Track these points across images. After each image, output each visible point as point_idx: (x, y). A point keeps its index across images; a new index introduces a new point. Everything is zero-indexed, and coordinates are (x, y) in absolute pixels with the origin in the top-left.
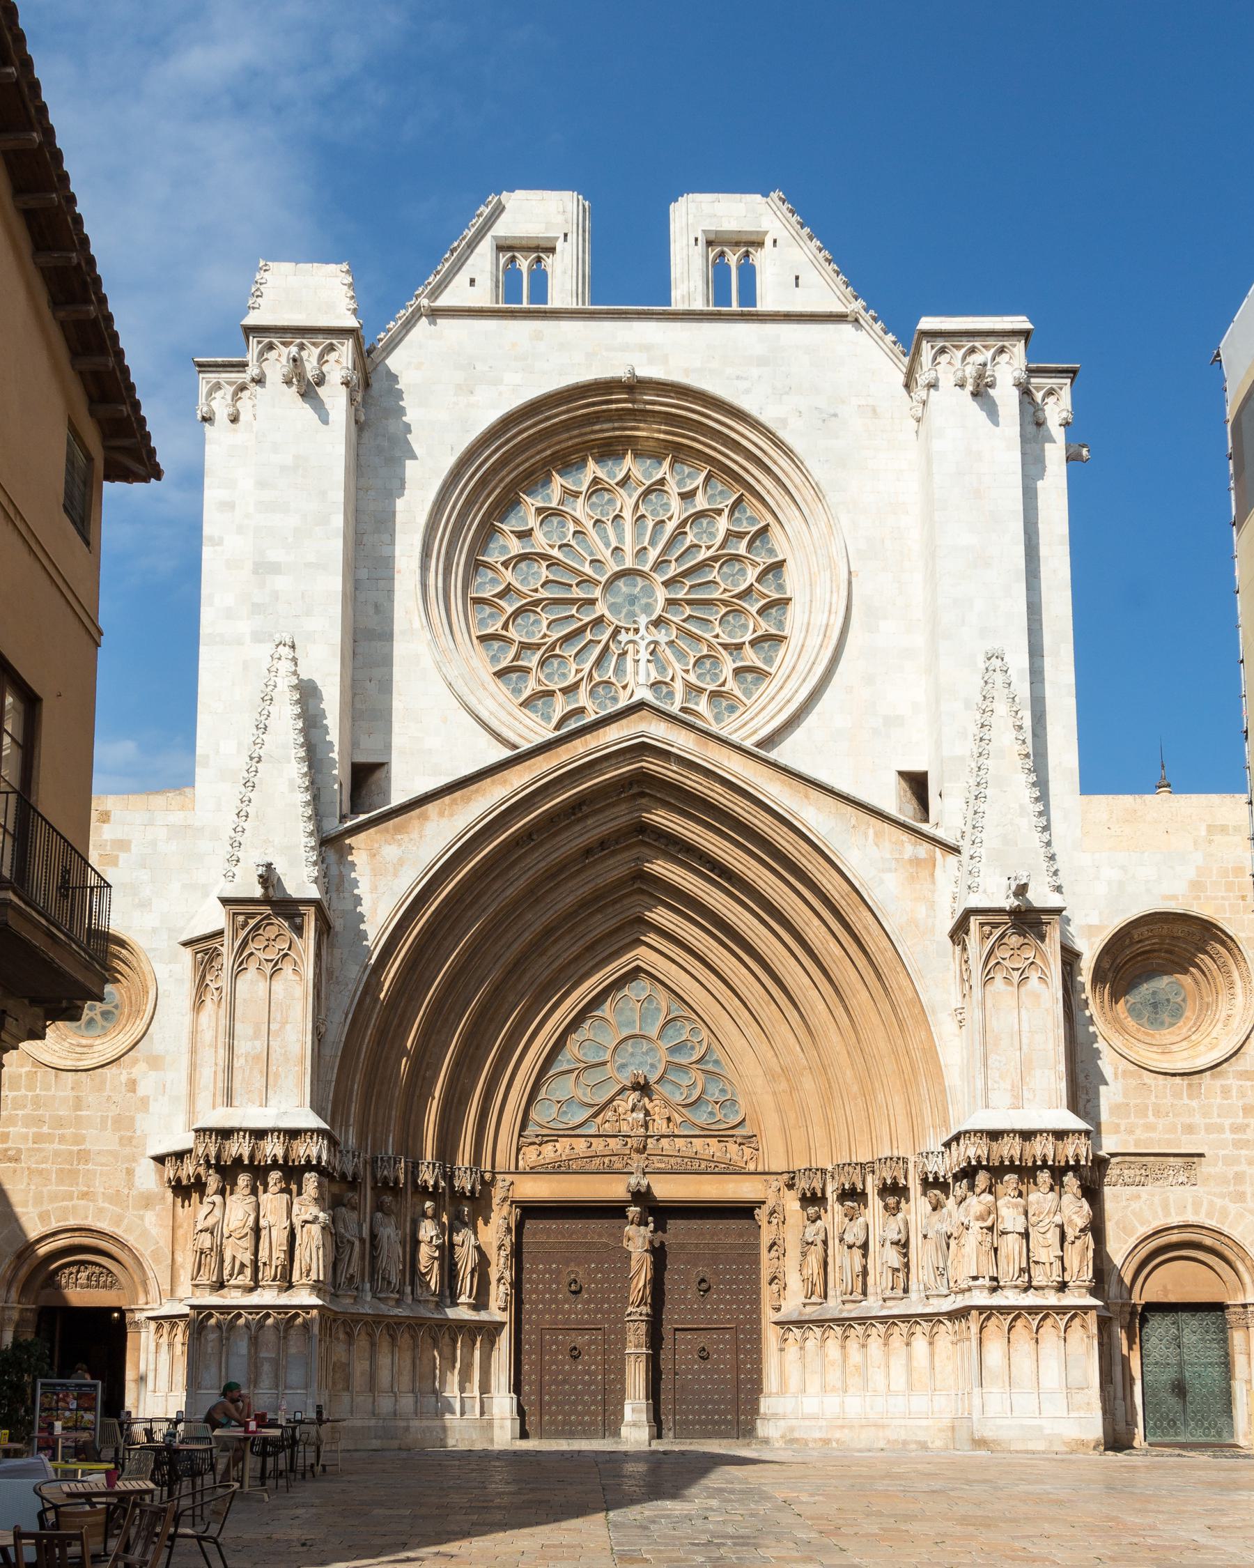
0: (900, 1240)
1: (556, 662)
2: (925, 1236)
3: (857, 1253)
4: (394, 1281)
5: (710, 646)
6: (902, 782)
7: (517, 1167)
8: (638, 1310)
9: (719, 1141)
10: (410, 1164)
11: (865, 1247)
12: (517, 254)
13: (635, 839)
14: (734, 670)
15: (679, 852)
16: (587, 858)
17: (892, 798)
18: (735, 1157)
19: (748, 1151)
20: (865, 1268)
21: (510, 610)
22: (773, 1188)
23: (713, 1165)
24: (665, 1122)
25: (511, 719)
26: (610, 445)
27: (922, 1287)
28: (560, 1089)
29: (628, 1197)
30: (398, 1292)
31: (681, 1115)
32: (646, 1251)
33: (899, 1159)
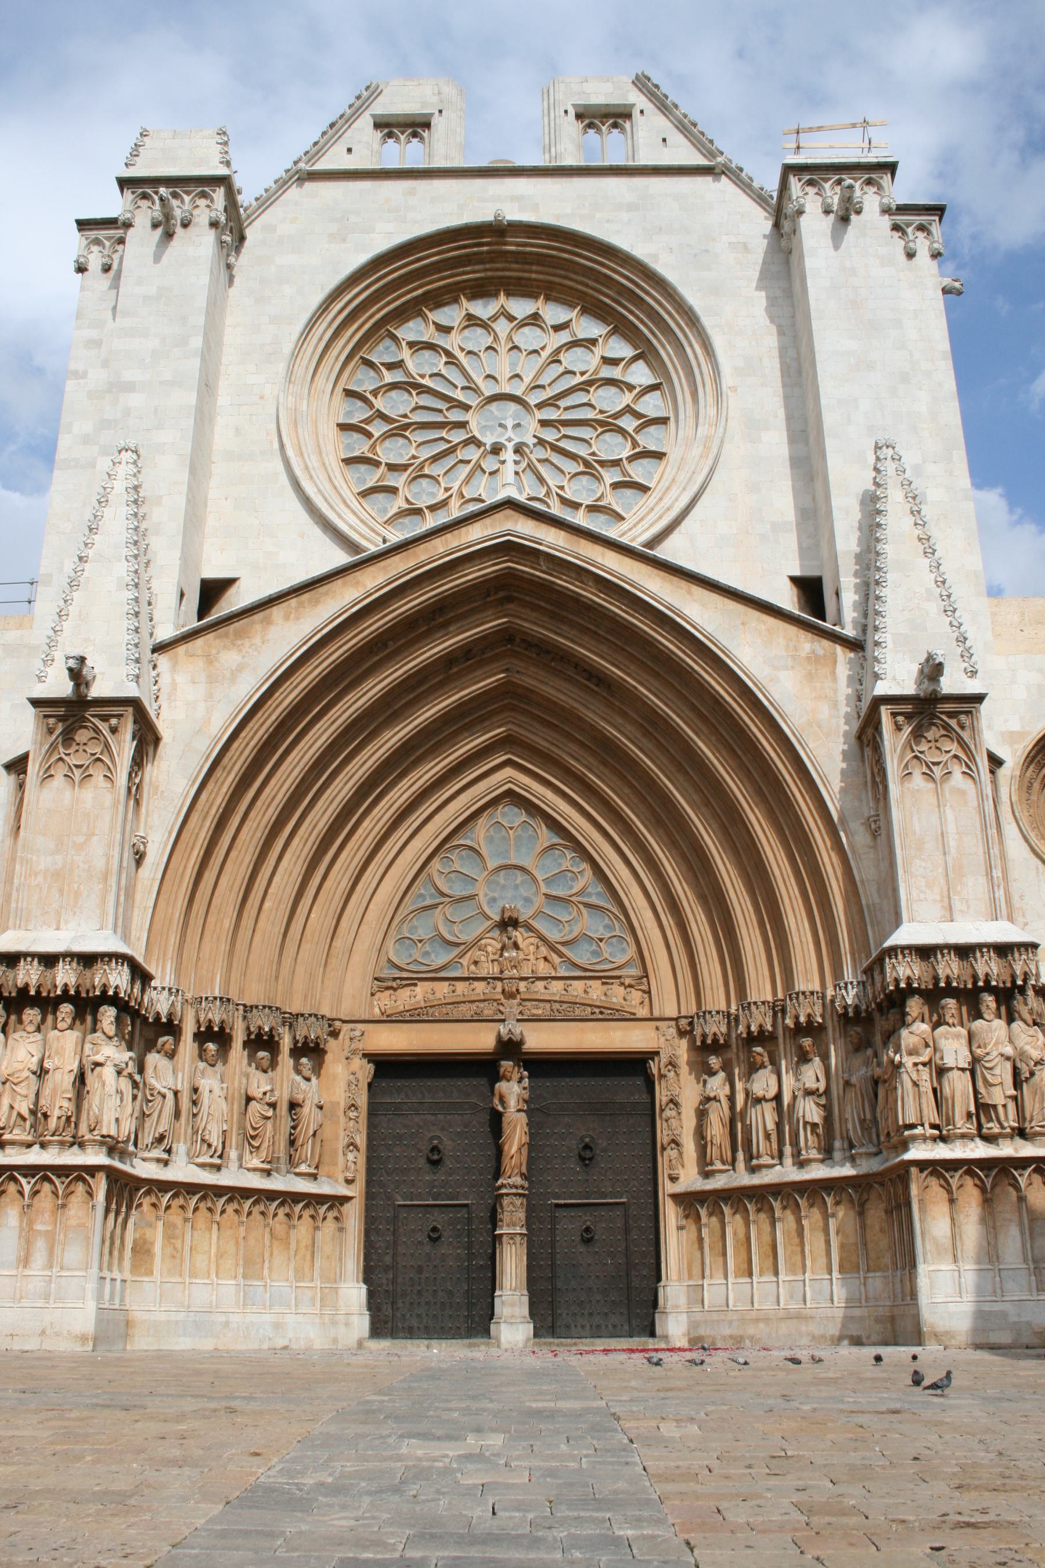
0: (818, 1089)
1: (424, 482)
2: (847, 1084)
4: (215, 1144)
5: (587, 464)
6: (795, 590)
8: (509, 1181)
9: (604, 983)
10: (241, 1008)
11: (778, 1098)
12: (395, 130)
13: (504, 648)
14: (611, 485)
15: (552, 660)
16: (450, 668)
17: (787, 599)
19: (636, 996)
21: (377, 435)
23: (597, 1010)
25: (373, 534)
26: (482, 286)
27: (846, 1145)
30: (221, 1157)
31: (561, 955)
32: (519, 1111)
33: (812, 993)
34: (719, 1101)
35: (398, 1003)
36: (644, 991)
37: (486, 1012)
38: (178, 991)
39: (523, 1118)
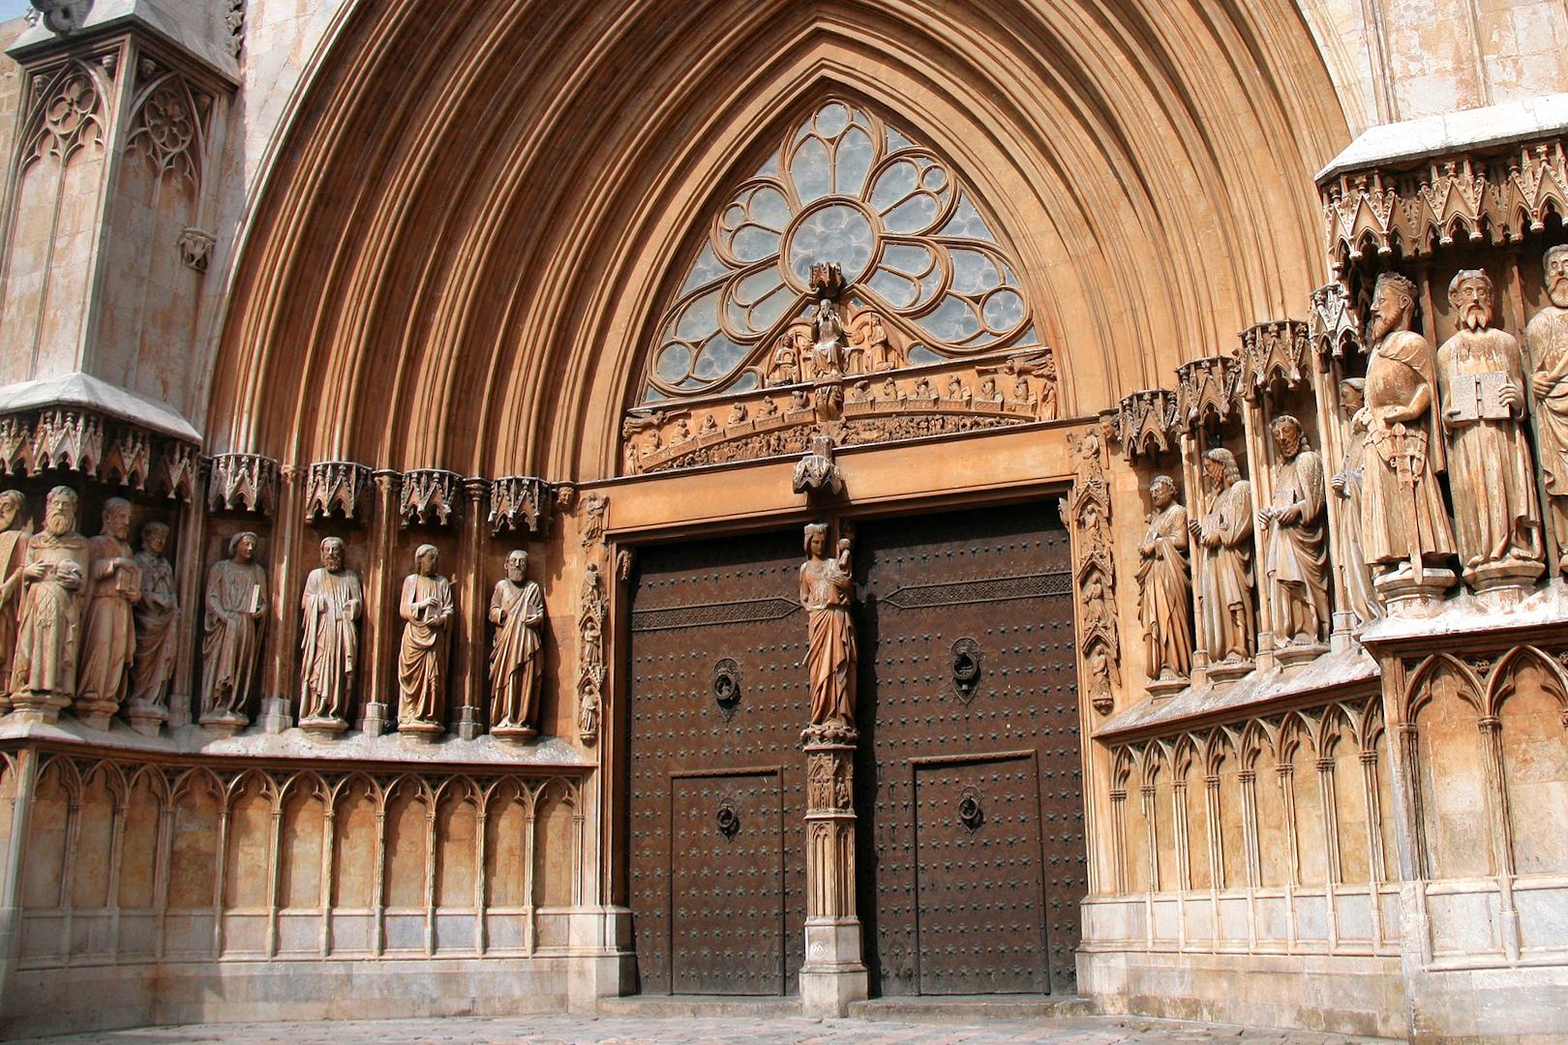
0: (1299, 514)
3: (1228, 562)
7: (619, 470)
9: (981, 373)
18: (1011, 400)
19: (1036, 385)
20: (1253, 592)
22: (1086, 452)
24: (879, 349)
28: (700, 321)
29: (799, 501)
31: (910, 333)
32: (831, 606)
34: (1161, 558)
35: (662, 448)
36: (1048, 377)
37: (789, 446)
38: (252, 460)
39: (839, 620)
